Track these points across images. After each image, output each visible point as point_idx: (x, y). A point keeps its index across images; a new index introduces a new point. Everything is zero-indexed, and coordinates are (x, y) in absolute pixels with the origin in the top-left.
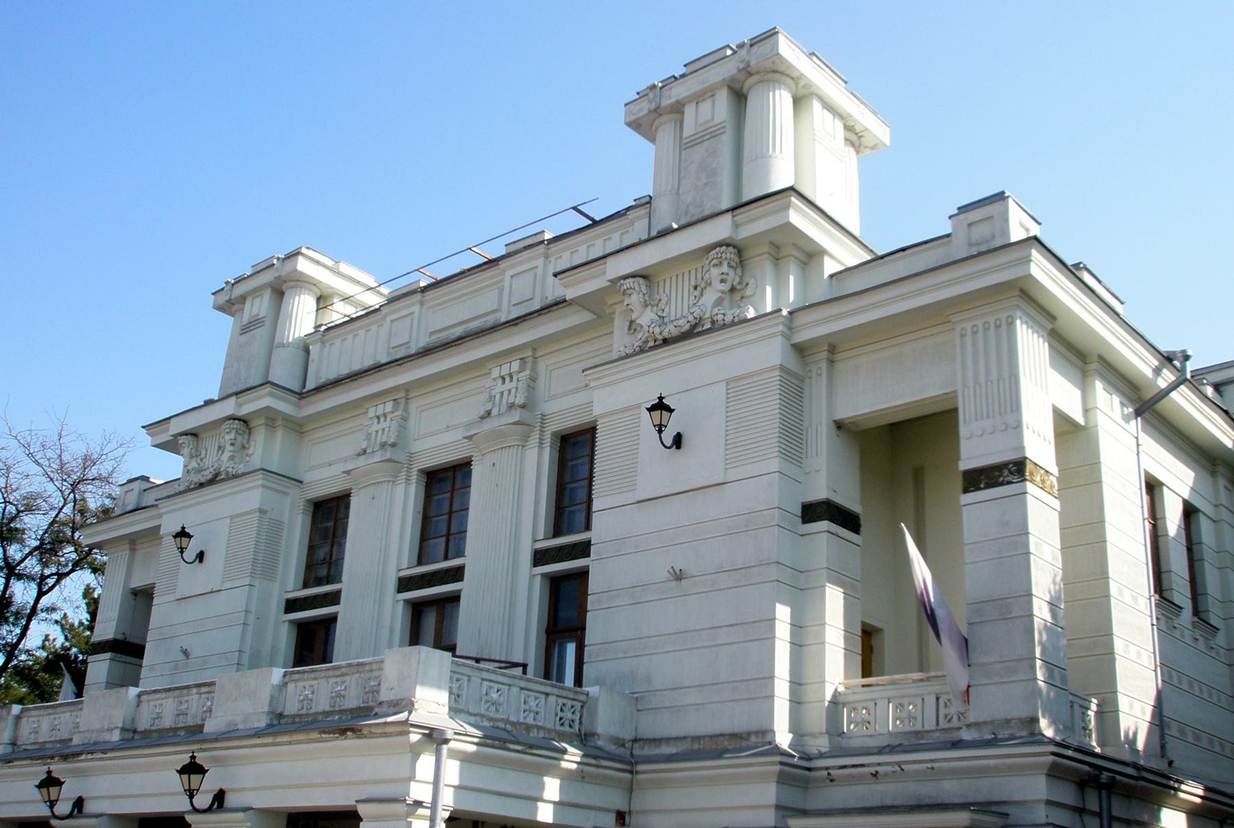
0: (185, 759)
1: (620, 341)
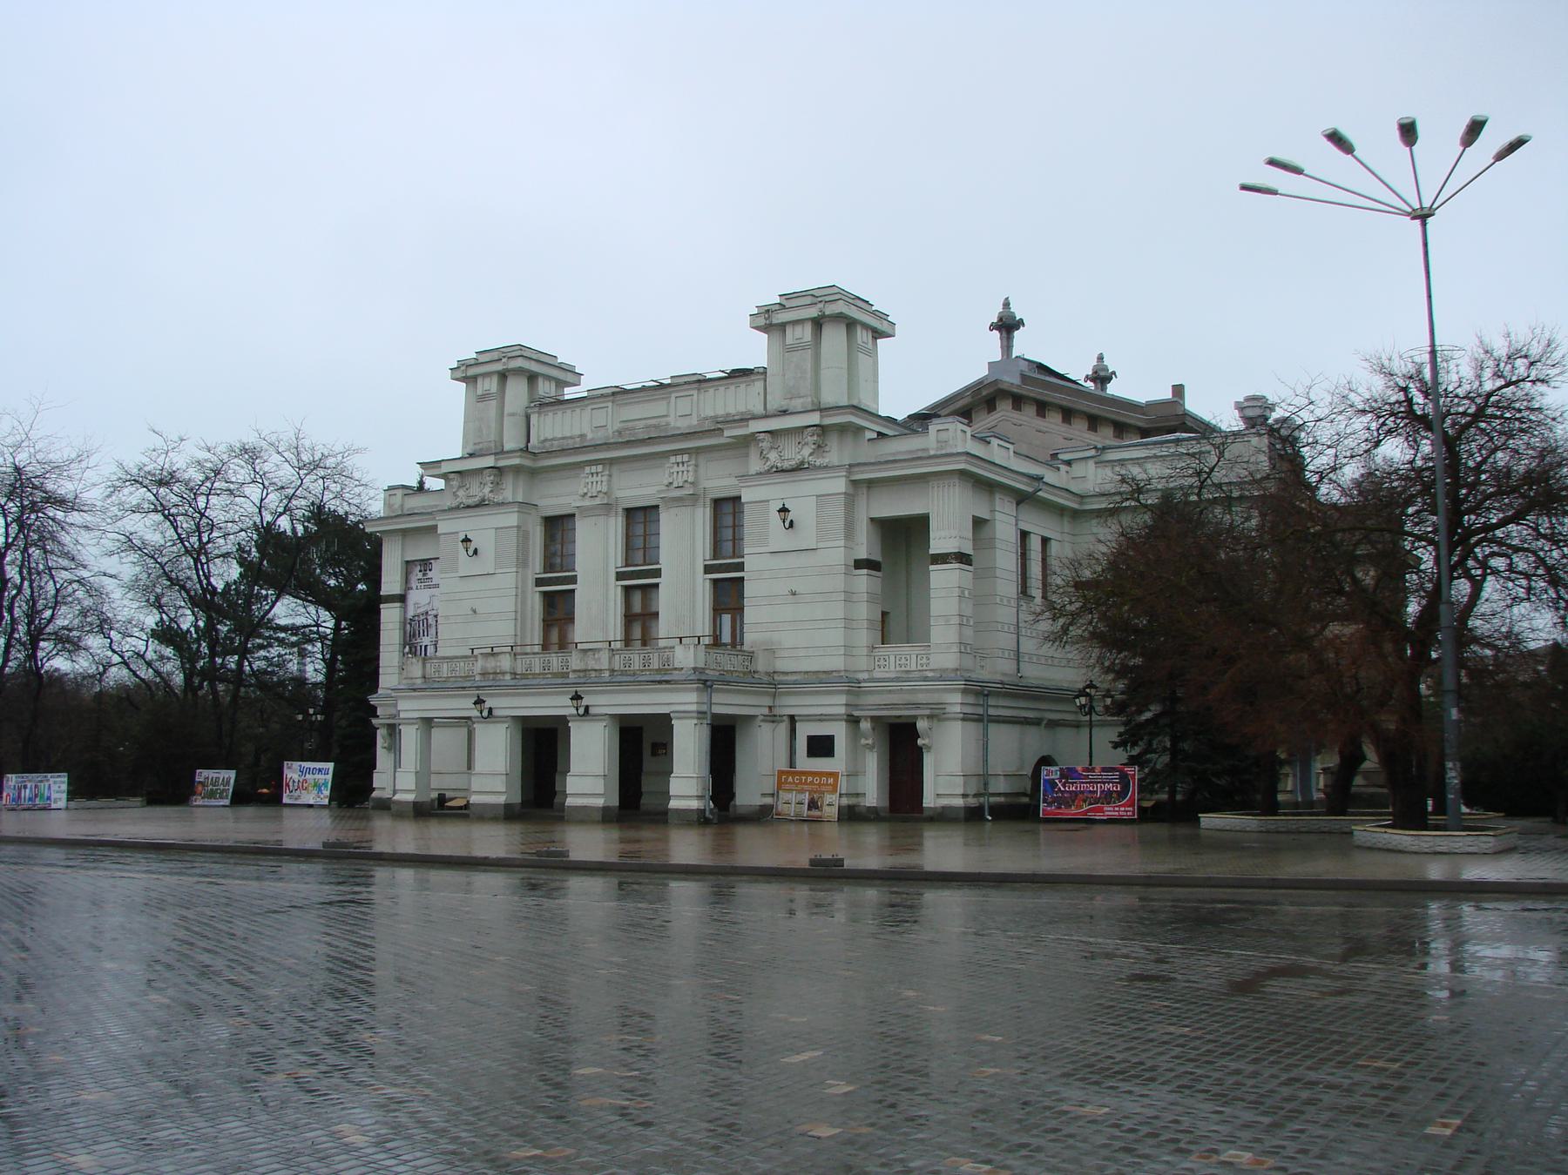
1: (755, 465)
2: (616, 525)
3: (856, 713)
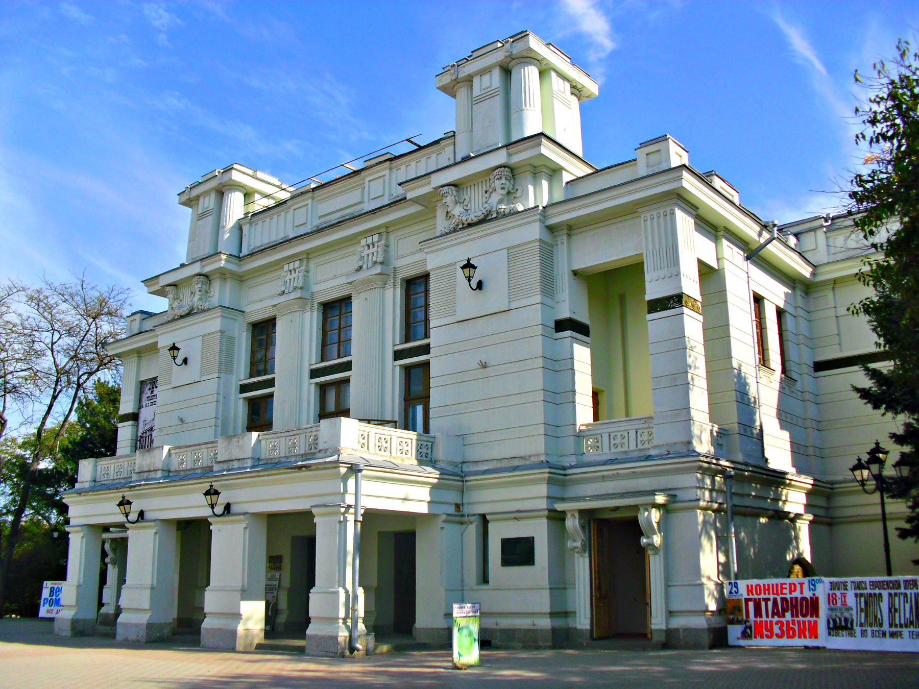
0: (206, 487)
1: (442, 224)
2: (311, 321)
3: (559, 506)
